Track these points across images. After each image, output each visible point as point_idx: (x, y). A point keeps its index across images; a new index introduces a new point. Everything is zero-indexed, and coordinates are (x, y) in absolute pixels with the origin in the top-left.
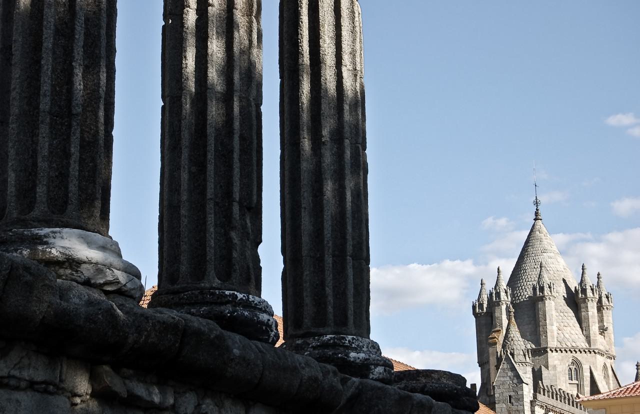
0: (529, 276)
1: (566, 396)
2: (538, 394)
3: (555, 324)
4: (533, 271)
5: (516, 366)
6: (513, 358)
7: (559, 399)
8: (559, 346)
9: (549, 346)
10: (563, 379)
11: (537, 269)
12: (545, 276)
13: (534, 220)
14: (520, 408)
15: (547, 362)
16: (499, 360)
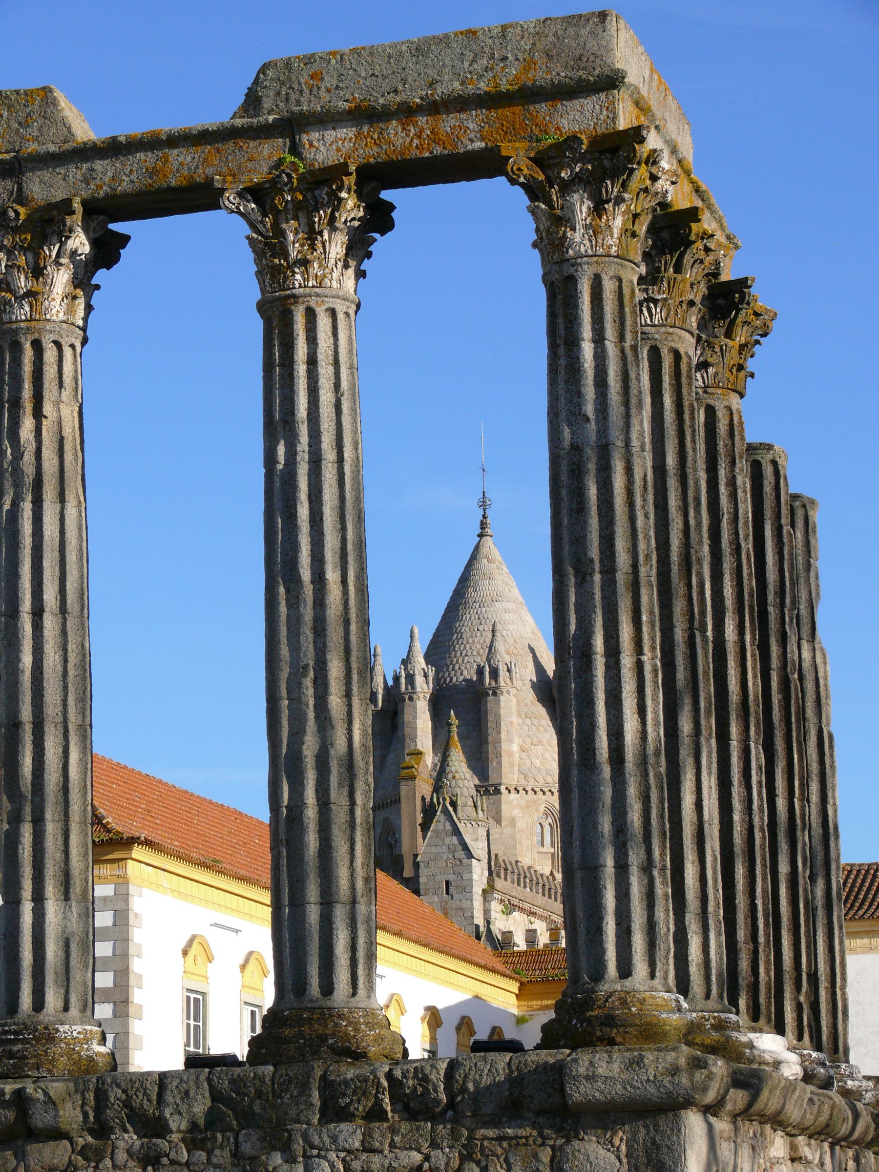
0: (468, 647)
1: (540, 878)
2: (496, 879)
3: (517, 741)
4: (476, 636)
5: (461, 826)
6: (455, 810)
7: (528, 885)
8: (523, 782)
9: (504, 781)
10: (526, 843)
11: (484, 634)
12: (500, 646)
13: (478, 536)
14: (465, 904)
15: (499, 811)
16: (429, 812)
